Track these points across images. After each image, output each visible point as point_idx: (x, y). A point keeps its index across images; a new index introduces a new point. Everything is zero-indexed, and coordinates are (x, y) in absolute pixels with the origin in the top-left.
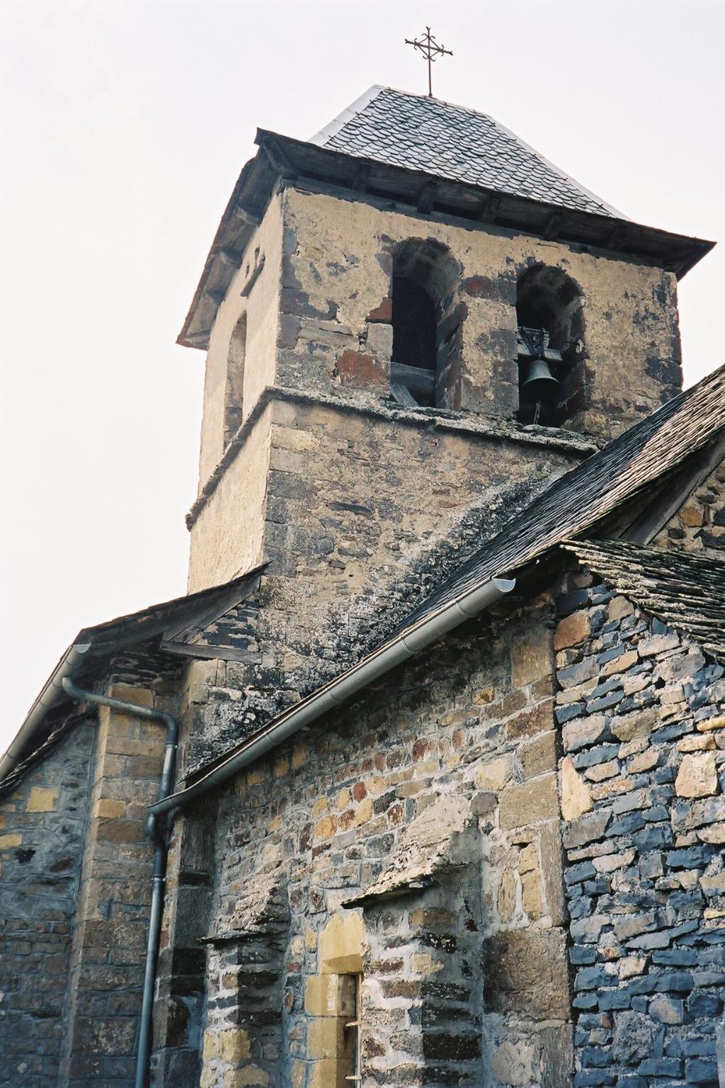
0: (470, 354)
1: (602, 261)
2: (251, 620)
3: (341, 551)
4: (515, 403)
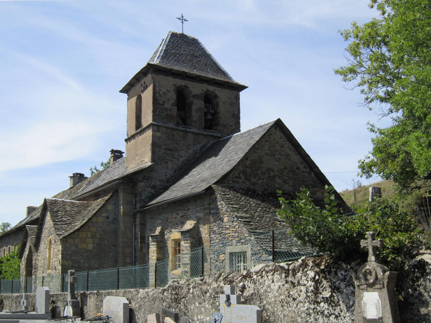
0: (194, 113)
1: (223, 90)
2: (149, 175)
3: (167, 160)
4: (203, 125)
